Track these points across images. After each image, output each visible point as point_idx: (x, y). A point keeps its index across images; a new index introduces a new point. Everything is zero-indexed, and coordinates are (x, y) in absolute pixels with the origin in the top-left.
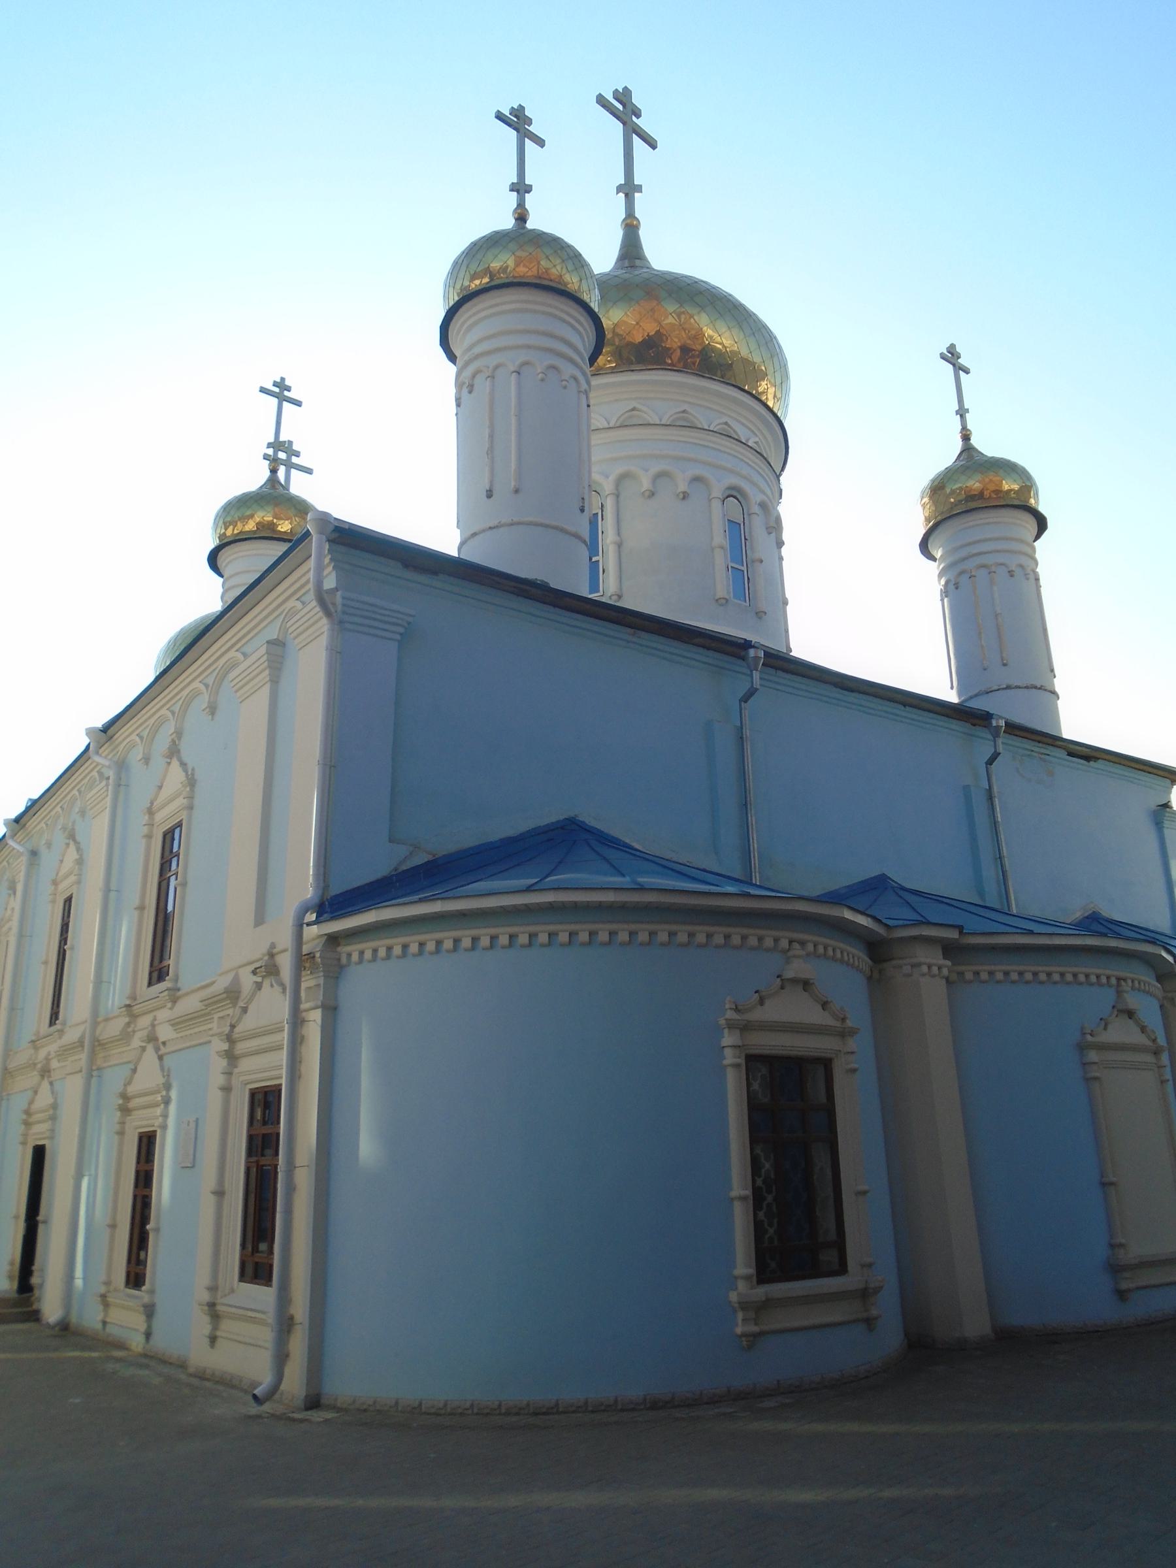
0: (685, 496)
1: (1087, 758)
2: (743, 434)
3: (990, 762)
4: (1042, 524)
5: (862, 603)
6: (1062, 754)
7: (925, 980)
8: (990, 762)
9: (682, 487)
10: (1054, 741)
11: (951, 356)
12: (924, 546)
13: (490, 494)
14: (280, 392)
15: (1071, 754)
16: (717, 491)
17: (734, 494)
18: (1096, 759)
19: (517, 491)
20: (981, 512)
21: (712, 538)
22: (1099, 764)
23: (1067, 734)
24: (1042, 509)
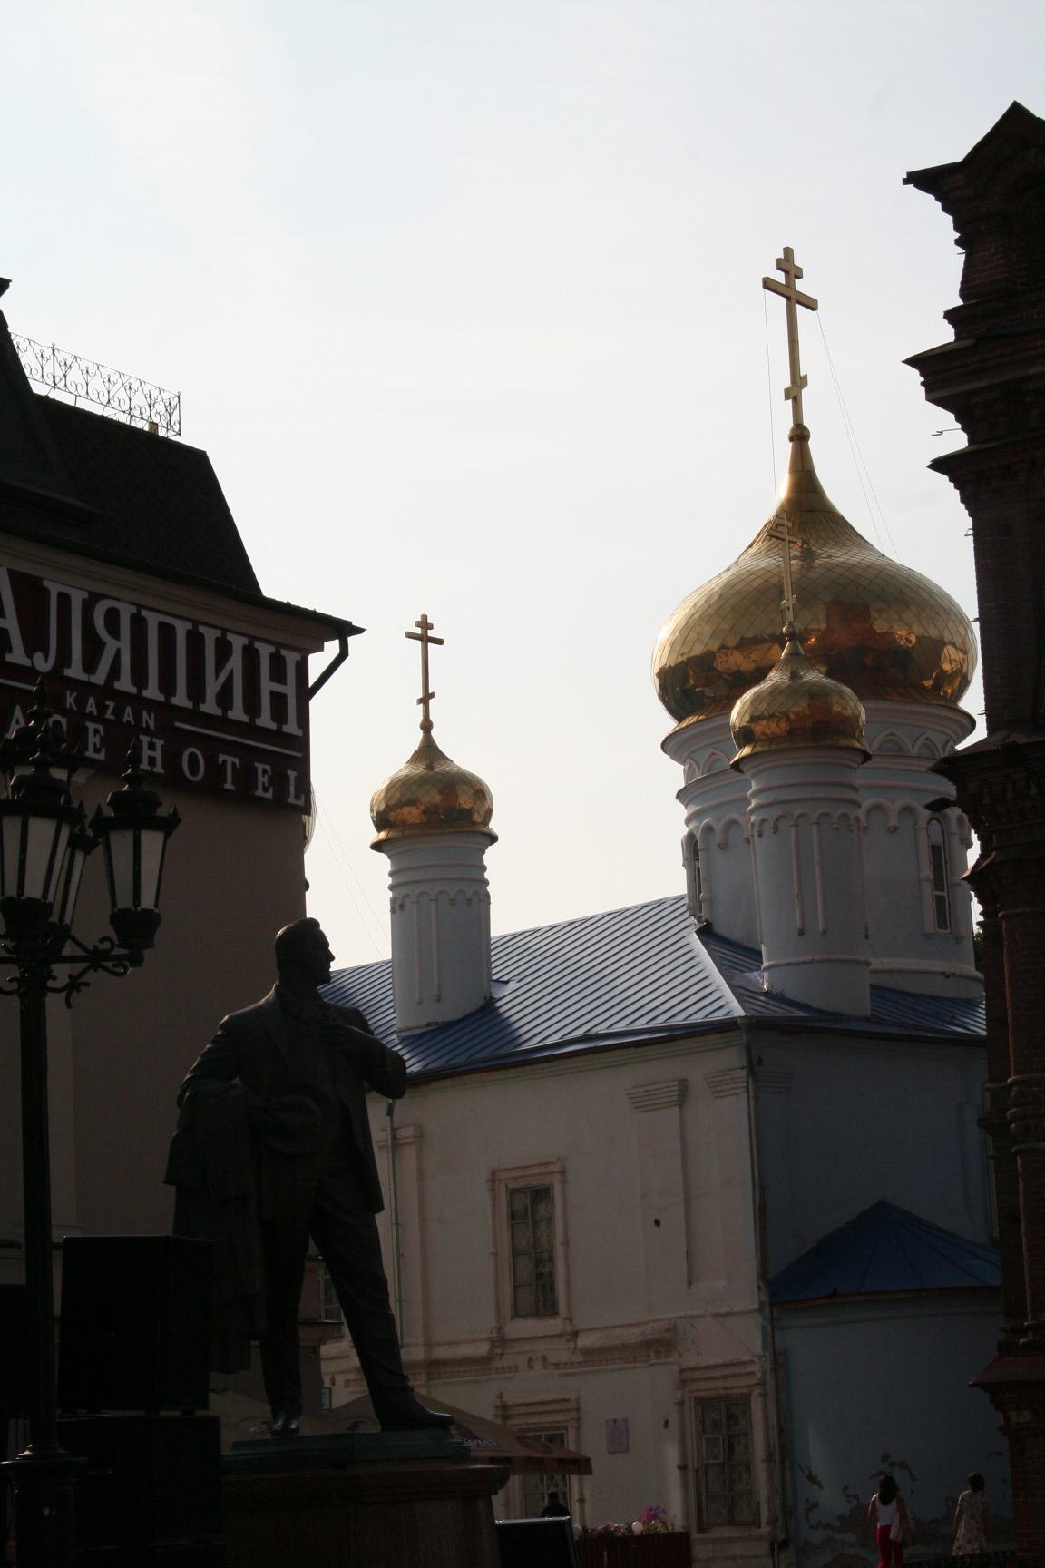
9: (893, 822)
13: (801, 933)
19: (824, 932)
21: (919, 870)
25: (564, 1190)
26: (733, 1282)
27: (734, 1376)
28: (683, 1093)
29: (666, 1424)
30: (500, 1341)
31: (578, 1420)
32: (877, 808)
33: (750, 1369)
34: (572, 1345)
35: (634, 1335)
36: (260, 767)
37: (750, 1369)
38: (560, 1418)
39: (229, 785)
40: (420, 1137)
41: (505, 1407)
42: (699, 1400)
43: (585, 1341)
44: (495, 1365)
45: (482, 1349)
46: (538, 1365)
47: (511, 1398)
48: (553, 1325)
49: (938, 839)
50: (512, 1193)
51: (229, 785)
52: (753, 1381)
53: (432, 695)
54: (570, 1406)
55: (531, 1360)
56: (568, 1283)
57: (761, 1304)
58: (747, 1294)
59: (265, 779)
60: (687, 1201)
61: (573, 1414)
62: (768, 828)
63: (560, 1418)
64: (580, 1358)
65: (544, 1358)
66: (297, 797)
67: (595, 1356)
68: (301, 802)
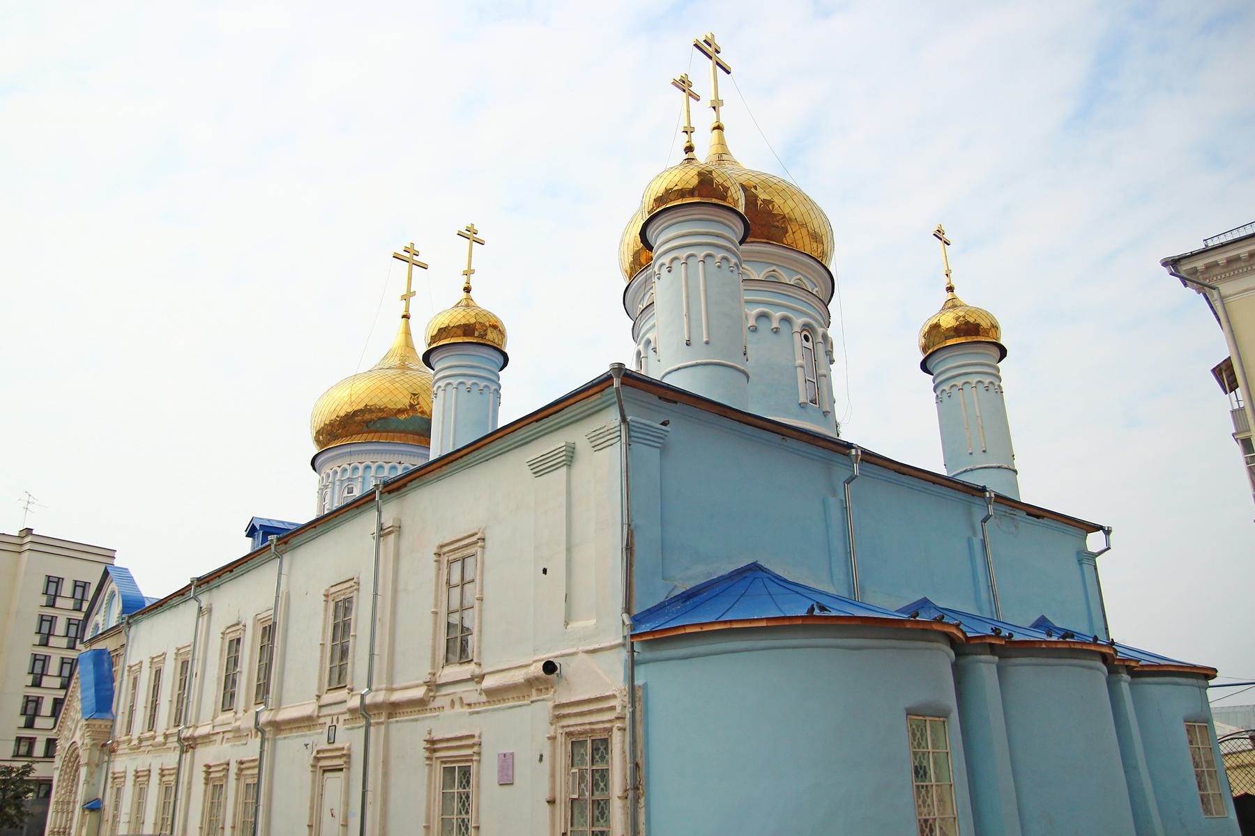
0: (776, 331)
1: (1038, 517)
3: (985, 521)
4: (1003, 352)
5: (885, 406)
8: (985, 521)
9: (775, 324)
10: (1011, 504)
11: (939, 234)
12: (924, 367)
14: (470, 235)
15: (1028, 514)
16: (797, 328)
17: (807, 327)
18: (1043, 517)
19: (707, 343)
20: (962, 345)
22: (1045, 521)
23: (1024, 499)
24: (1002, 342)
25: (483, 553)
26: (602, 621)
28: (570, 457)
29: (541, 760)
30: (433, 686)
31: (479, 754)
32: (763, 316)
34: (478, 687)
35: (518, 677)
38: (469, 752)
40: (398, 529)
41: (432, 742)
42: (569, 734)
43: (489, 682)
45: (419, 693)
46: (457, 705)
50: (450, 563)
53: (473, 272)
54: (476, 740)
55: (453, 702)
58: (614, 628)
61: (476, 749)
62: (664, 270)
63: (469, 752)
64: (484, 698)
67: (492, 693)
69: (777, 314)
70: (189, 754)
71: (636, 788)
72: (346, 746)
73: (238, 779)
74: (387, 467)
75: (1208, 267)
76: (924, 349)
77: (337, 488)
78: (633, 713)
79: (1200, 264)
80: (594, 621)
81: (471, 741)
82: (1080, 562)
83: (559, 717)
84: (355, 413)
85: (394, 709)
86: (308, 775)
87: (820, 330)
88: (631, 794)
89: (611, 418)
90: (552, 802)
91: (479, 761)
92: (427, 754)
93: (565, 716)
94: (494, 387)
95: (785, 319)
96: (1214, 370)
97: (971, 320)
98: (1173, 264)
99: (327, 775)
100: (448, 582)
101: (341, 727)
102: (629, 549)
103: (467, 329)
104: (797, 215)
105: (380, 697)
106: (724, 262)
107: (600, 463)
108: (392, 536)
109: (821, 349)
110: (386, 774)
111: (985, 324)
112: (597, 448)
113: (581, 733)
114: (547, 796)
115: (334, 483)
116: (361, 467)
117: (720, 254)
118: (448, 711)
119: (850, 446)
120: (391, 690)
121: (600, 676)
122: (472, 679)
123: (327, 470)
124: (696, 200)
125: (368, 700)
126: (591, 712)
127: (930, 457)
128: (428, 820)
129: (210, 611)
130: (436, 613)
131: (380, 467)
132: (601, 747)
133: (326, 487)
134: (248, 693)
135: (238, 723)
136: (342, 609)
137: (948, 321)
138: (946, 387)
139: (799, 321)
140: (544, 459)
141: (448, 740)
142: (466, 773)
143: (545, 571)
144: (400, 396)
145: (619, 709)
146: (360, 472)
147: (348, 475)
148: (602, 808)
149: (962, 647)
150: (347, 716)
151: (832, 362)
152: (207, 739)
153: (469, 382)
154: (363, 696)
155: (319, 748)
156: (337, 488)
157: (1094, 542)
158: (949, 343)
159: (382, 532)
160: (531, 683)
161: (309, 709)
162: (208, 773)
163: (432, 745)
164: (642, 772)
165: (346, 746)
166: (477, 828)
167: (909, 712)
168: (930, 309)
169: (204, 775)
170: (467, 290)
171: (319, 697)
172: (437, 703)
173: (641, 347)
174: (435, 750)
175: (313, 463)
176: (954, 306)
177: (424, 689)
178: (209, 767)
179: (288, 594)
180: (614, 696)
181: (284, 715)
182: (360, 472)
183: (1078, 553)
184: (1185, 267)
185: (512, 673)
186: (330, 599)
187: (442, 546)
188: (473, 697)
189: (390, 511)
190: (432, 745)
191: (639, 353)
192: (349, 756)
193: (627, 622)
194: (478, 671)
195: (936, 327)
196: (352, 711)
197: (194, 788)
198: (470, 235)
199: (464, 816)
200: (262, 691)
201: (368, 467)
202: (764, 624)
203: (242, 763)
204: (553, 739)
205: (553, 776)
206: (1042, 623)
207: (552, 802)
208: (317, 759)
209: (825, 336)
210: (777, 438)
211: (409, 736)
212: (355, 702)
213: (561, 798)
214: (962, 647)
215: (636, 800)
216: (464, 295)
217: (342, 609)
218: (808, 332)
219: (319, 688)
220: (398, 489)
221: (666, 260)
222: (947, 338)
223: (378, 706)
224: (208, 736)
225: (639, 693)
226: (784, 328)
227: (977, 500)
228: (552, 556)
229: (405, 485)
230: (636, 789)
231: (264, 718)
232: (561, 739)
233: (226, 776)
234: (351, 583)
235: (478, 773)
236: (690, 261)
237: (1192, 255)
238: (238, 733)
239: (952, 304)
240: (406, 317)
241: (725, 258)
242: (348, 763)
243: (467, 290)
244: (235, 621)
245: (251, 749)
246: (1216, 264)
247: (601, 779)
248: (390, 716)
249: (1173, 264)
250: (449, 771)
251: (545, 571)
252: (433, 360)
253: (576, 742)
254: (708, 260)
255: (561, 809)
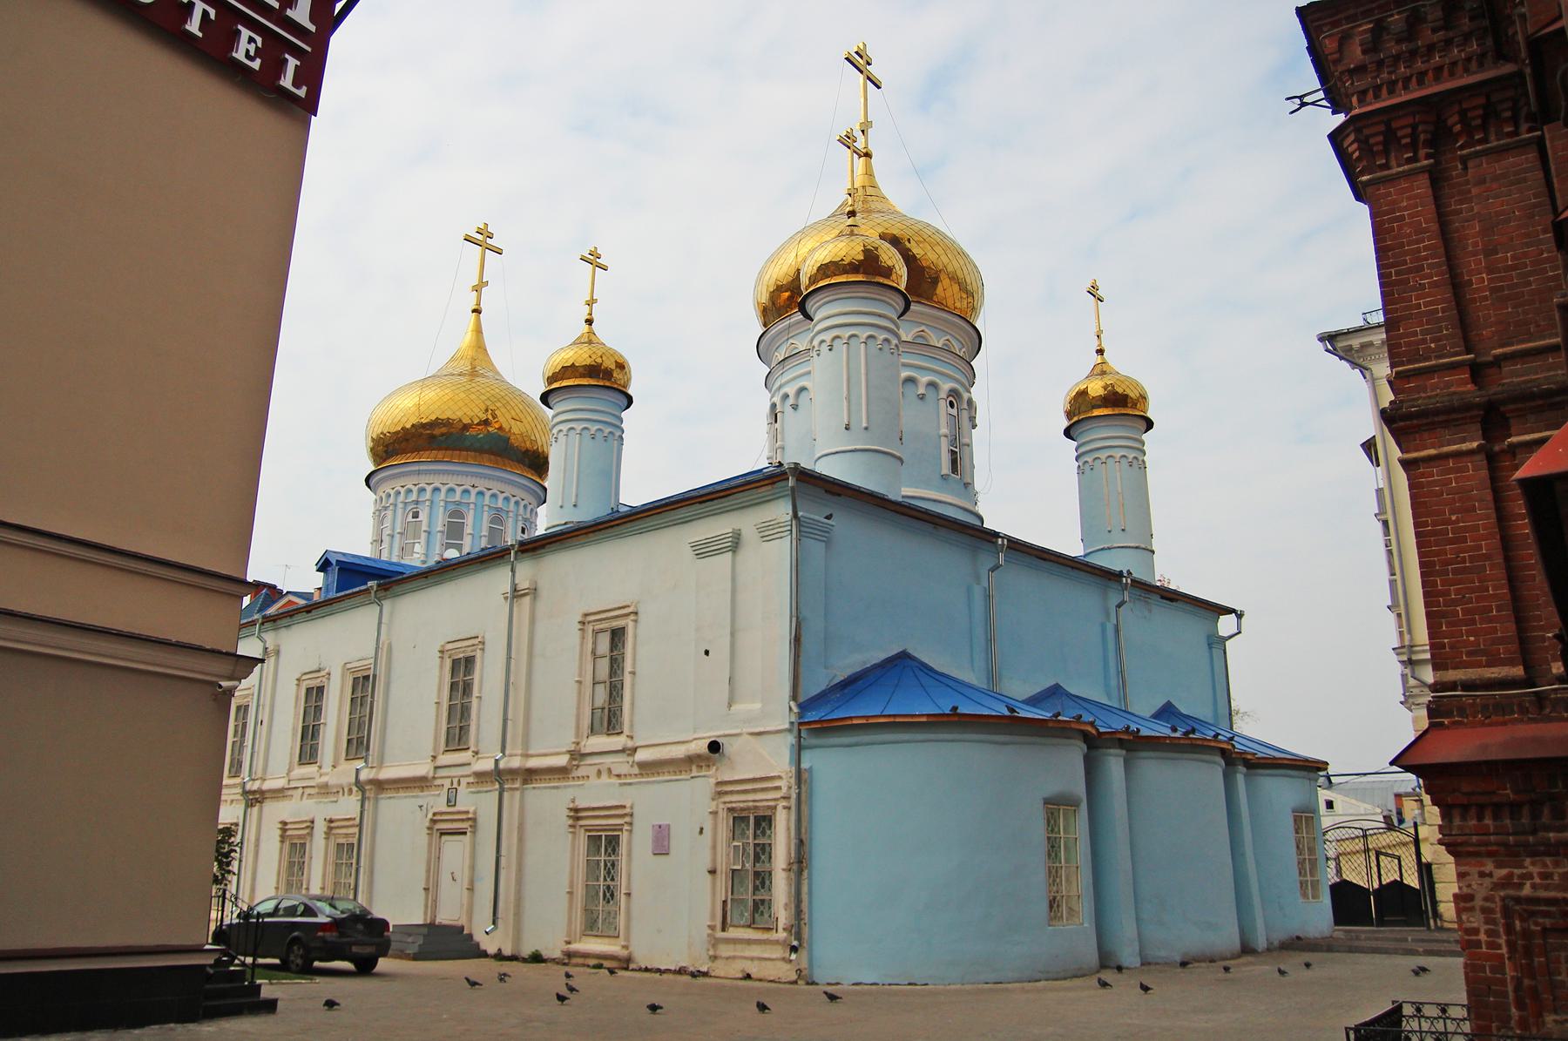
0: (922, 397)
1: (1171, 600)
2: (956, 347)
3: (1119, 606)
4: (1149, 425)
6: (1157, 597)
7: (1114, 764)
8: (1119, 606)
9: (921, 390)
11: (1093, 291)
12: (1068, 433)
16: (943, 395)
17: (954, 393)
20: (1108, 413)
21: (939, 428)
24: (1149, 415)
26: (767, 704)
27: (763, 790)
28: (735, 544)
30: (577, 755)
31: (631, 824)
33: (777, 783)
34: (630, 759)
35: (679, 752)
36: (246, 33)
37: (777, 783)
39: (194, 26)
40: (534, 591)
41: (576, 810)
42: (730, 810)
43: (641, 756)
44: (575, 774)
45: (562, 761)
46: (604, 776)
47: (581, 804)
48: (617, 742)
49: (954, 412)
50: (596, 633)
51: (194, 26)
52: (778, 795)
54: (627, 811)
55: (599, 773)
56: (633, 704)
57: (792, 723)
58: (781, 714)
59: (252, 48)
60: (733, 634)
61: (627, 819)
64: (636, 770)
65: (610, 770)
66: (296, 84)
68: (302, 92)
69: (924, 379)
70: (256, 809)
71: (800, 862)
72: (472, 809)
73: (327, 838)
74: (459, 490)
75: (1364, 346)
76: (1069, 415)
77: (400, 511)
78: (799, 795)
79: (1355, 342)
80: (757, 706)
81: (623, 812)
82: (1210, 646)
83: (720, 794)
84: (423, 426)
85: (530, 775)
86: (423, 838)
87: (966, 396)
88: (795, 867)
89: (781, 511)
90: (713, 872)
91: (630, 831)
92: (570, 822)
93: (726, 793)
94: (618, 433)
95: (932, 385)
96: (1363, 445)
97: (1120, 390)
98: (1330, 339)
99: (444, 838)
100: (594, 652)
101: (463, 790)
102: (797, 641)
103: (593, 370)
104: (950, 269)
105: (516, 763)
106: (886, 347)
107: (767, 549)
108: (527, 599)
109: (965, 415)
110: (521, 840)
111: (1133, 394)
112: (766, 538)
113: (743, 809)
114: (709, 866)
115: (395, 505)
116: (429, 489)
117: (882, 336)
118: (593, 781)
119: (996, 535)
120: (527, 756)
121: (766, 758)
122: (623, 751)
123: (387, 488)
124: (860, 278)
125: (502, 765)
126: (754, 791)
127: (1072, 547)
128: (571, 886)
129: (278, 653)
130: (580, 682)
131: (451, 490)
132: (764, 822)
133: (386, 508)
134: (336, 748)
135: (324, 779)
136: (462, 669)
137: (1096, 388)
138: (1089, 458)
139: (946, 386)
140: (708, 542)
141: (594, 809)
142: (613, 843)
143: (707, 653)
144: (476, 410)
145: (784, 789)
146: (428, 495)
147: (414, 497)
148: (762, 880)
149: (1095, 742)
150: (471, 780)
151: (974, 426)
152: (279, 794)
153: (594, 428)
154: (497, 761)
155: (436, 810)
156: (400, 511)
157: (1226, 625)
158: (1096, 412)
159: (516, 594)
160: (691, 760)
161: (423, 769)
162: (284, 830)
163: (576, 814)
164: (806, 848)
165: (472, 809)
166: (628, 894)
167: (1047, 802)
168: (1075, 373)
169: (279, 832)
170: (589, 322)
171: (434, 757)
172: (581, 772)
173: (777, 399)
174: (578, 819)
175: (367, 480)
176: (1103, 373)
177: (567, 757)
178: (285, 823)
179: (390, 646)
180: (780, 777)
181: (386, 774)
182: (428, 495)
183: (1209, 637)
184: (1340, 344)
185: (668, 748)
186: (446, 655)
187: (586, 615)
188: (624, 769)
189: (526, 571)
190: (576, 814)
191: (774, 406)
192: (474, 820)
193: (795, 710)
194: (630, 744)
195: (1083, 394)
196: (481, 776)
197: (263, 845)
198: (593, 260)
199: (609, 882)
200: (358, 745)
201: (437, 489)
202: (924, 719)
203: (331, 821)
204: (714, 813)
205: (714, 847)
206: (1167, 712)
207: (713, 872)
208: (434, 821)
209: (970, 402)
210: (929, 527)
211: (549, 803)
212: (486, 765)
213: (722, 867)
214: (1095, 742)
215: (800, 872)
216: (586, 328)
217: (462, 669)
218: (954, 397)
219: (435, 749)
220: (534, 549)
221: (827, 336)
222: (1094, 407)
223: (513, 772)
224: (282, 790)
225: (805, 776)
226: (931, 394)
227: (1114, 585)
228: (720, 644)
229: (543, 547)
230: (800, 862)
231: (363, 776)
232: (722, 814)
233: (311, 835)
234: (475, 641)
235: (630, 843)
236: (853, 341)
237: (1349, 333)
238: (325, 790)
239: (1101, 371)
240: (477, 311)
241: (886, 340)
242: (474, 827)
243: (589, 322)
244: (315, 668)
245: (348, 806)
246: (1371, 344)
247: (763, 852)
248: (525, 782)
249: (1330, 339)
250: (594, 841)
251: (707, 653)
252: (551, 400)
253: (739, 819)
254: (870, 342)
255: (722, 880)
